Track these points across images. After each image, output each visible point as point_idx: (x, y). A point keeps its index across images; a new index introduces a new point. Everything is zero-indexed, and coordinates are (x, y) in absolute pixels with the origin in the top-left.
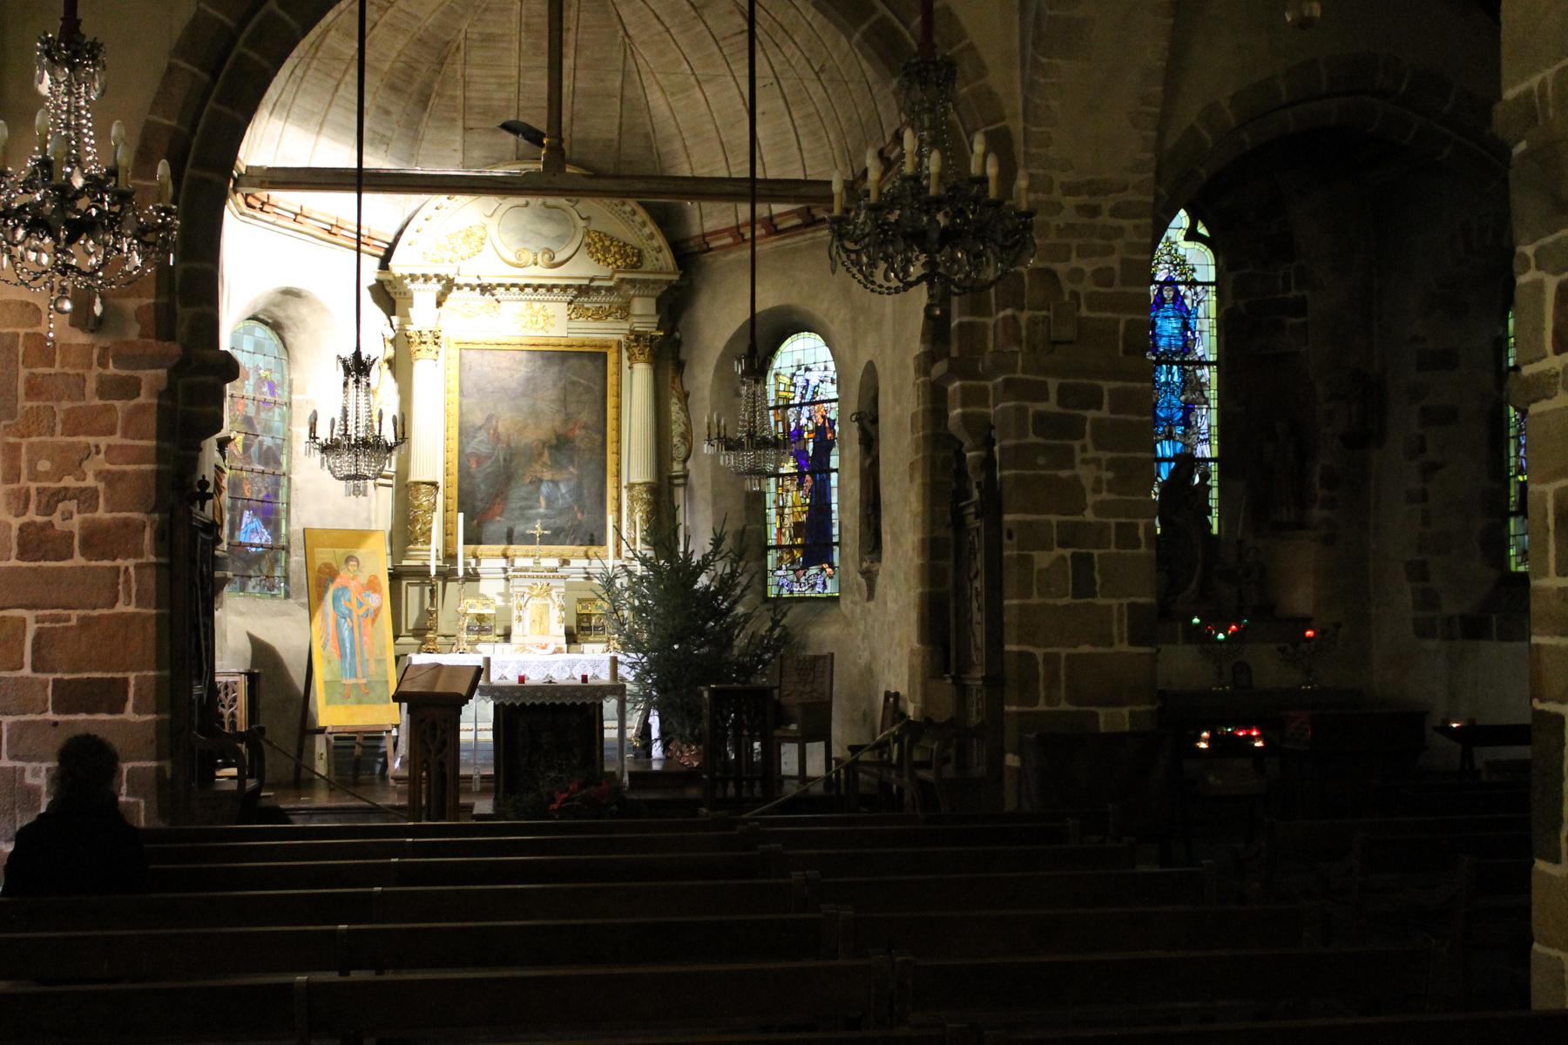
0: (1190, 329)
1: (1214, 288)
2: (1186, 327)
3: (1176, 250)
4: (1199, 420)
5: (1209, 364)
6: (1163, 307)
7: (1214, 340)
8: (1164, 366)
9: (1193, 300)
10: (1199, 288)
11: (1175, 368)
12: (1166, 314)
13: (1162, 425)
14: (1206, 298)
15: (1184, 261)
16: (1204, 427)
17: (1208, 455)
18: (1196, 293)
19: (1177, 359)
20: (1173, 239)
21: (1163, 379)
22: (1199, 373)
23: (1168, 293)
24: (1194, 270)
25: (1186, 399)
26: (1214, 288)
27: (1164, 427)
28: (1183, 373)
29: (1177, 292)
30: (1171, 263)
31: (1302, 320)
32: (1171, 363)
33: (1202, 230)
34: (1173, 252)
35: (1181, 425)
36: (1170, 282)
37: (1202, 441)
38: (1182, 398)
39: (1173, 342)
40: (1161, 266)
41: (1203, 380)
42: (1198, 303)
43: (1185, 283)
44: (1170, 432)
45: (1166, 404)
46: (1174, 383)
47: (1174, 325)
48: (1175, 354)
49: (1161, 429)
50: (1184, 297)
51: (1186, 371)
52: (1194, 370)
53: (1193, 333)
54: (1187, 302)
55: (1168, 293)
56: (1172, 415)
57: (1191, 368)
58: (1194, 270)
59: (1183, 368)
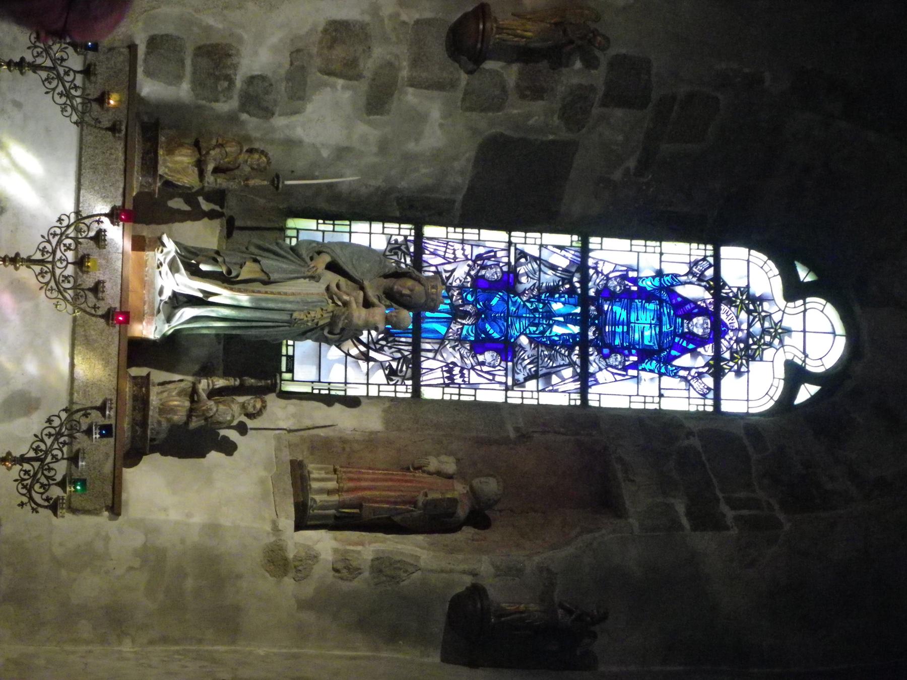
0: (641, 361)
1: (710, 409)
2: (646, 354)
3: (770, 345)
4: (485, 369)
5: (584, 392)
6: (677, 315)
7: (621, 403)
8: (578, 310)
9: (689, 369)
10: (709, 381)
11: (576, 329)
12: (665, 319)
13: (477, 301)
14: (693, 393)
15: (754, 359)
16: (474, 378)
17: (425, 379)
18: (700, 375)
19: (591, 335)
20: (787, 340)
21: (557, 307)
22: (568, 372)
23: (699, 326)
24: (739, 373)
25: (522, 348)
26: (710, 409)
27: (474, 304)
28: (568, 343)
29: (700, 341)
30: (750, 335)
31: (685, 521)
32: (584, 321)
33: (806, 392)
34: (768, 338)
35: (477, 335)
36: (718, 330)
37: (450, 371)
38: (524, 340)
39: (619, 329)
40: (743, 316)
41: (555, 379)
42: (684, 379)
43: (717, 356)
44: (466, 315)
45: (513, 309)
46: (550, 326)
47: (647, 333)
48: (600, 329)
49: (469, 298)
50: (694, 353)
51: (571, 349)
52: (572, 364)
53: (634, 366)
54: (685, 360)
55: (699, 326)
56: (495, 320)
57: (575, 358)
58: (739, 373)
59: (576, 344)
